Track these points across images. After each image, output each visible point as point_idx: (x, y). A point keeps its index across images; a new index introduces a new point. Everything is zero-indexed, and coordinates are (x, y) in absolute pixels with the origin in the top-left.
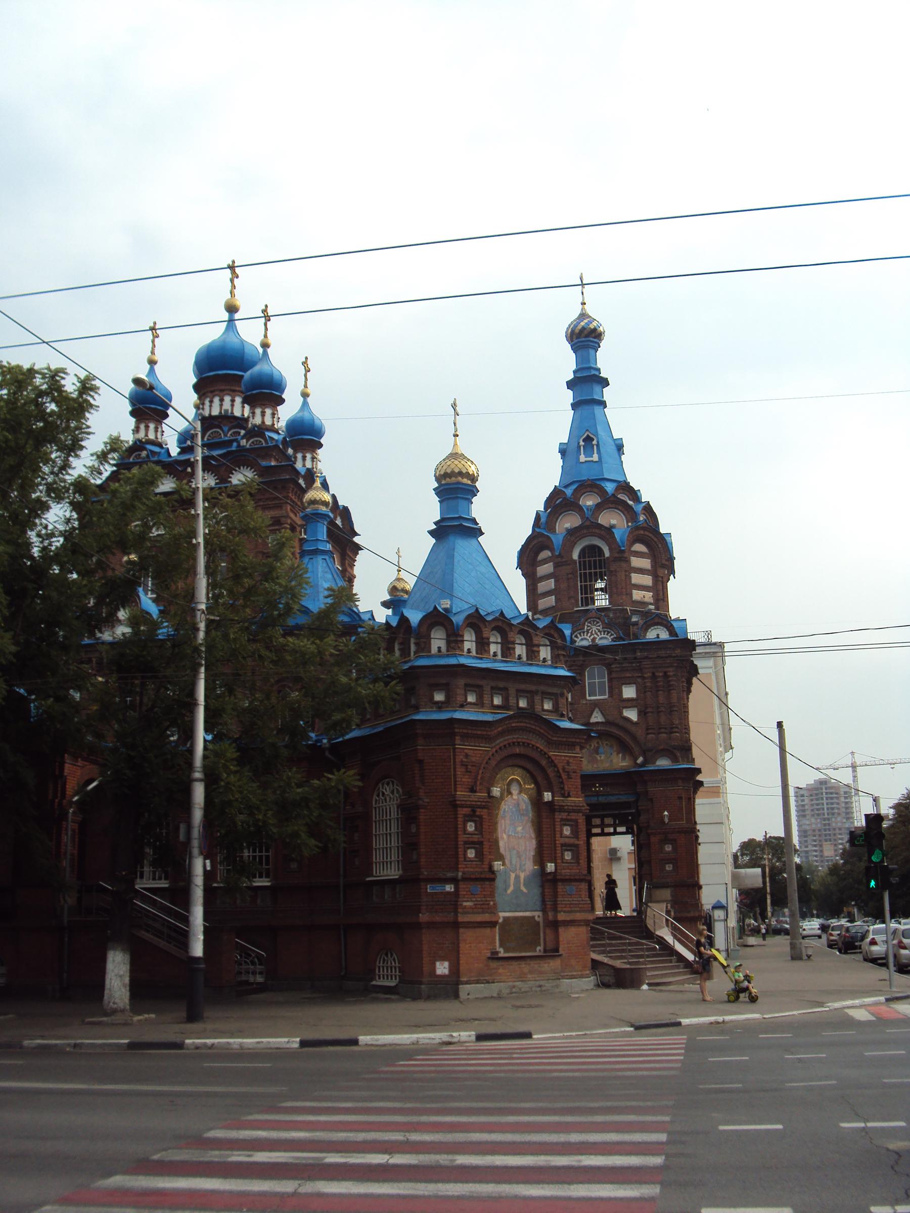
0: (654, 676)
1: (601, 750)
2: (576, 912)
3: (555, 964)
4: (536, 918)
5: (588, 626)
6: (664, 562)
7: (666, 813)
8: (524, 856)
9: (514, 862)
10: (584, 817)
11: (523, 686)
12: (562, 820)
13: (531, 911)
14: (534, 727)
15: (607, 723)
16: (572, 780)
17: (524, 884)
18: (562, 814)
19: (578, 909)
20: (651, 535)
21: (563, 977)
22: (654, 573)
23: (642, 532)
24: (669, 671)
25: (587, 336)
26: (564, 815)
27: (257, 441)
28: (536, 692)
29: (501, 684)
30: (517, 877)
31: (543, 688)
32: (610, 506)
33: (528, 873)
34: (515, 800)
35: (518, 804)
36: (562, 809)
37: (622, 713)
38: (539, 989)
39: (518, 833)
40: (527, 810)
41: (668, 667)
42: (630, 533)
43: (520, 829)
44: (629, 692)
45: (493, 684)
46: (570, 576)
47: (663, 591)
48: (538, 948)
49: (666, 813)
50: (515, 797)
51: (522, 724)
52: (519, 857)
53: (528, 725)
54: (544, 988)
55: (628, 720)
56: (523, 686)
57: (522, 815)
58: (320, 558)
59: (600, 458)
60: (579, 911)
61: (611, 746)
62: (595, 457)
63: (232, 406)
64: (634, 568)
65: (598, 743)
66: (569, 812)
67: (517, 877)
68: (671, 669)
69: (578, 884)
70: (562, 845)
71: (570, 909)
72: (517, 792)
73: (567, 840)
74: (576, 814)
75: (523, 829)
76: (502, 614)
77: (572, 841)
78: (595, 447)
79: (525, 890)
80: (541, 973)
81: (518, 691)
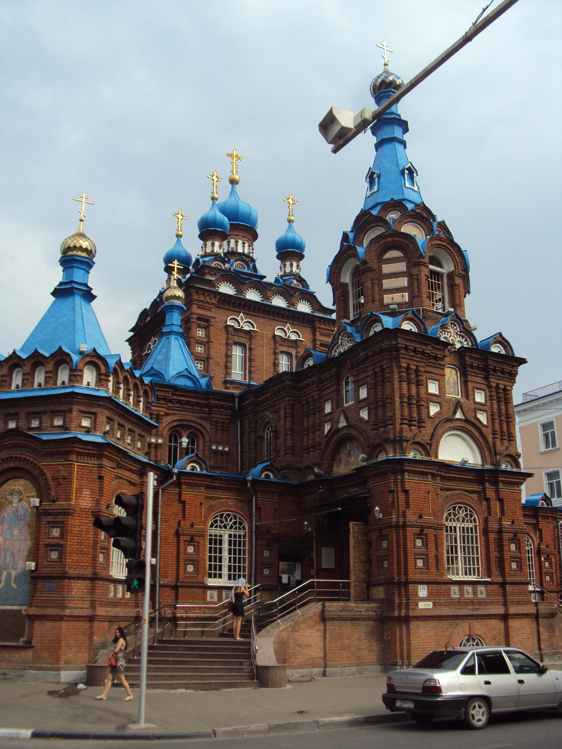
0: (375, 373)
1: (352, 453)
2: (48, 607)
3: (28, 655)
4: (23, 612)
5: (342, 339)
6: (416, 260)
7: (377, 508)
8: (18, 555)
9: (7, 562)
10: (93, 519)
11: (32, 409)
12: (49, 523)
13: (19, 605)
14: (25, 443)
15: (349, 426)
16: (63, 486)
17: (15, 582)
18: (49, 517)
19: (55, 605)
20: (399, 239)
21: (30, 668)
22: (408, 274)
23: (390, 239)
24: (383, 365)
25: (379, 90)
26: (50, 518)
27: (242, 265)
28: (45, 412)
29: (12, 411)
30: (9, 575)
31: (52, 408)
32: (372, 225)
33: (19, 571)
34: (14, 507)
35: (17, 511)
36: (46, 513)
37: (359, 414)
38: (3, 676)
39: (14, 536)
40: (25, 515)
41: (382, 360)
42: (428, 243)
43: (16, 532)
44: (363, 393)
45: (6, 411)
46: (341, 298)
47: (418, 288)
48: (22, 639)
49: (377, 508)
50: (15, 505)
51: (14, 442)
52: (13, 556)
53: (20, 442)
54: (7, 677)
55: (362, 419)
56: (32, 409)
57: (20, 520)
58: (173, 337)
59: (378, 187)
60: (53, 607)
61: (358, 448)
62: (376, 188)
63: (237, 245)
64: (386, 275)
65: (350, 446)
66: (56, 515)
67: (9, 575)
68: (384, 362)
69: (58, 581)
70: (47, 545)
71: (45, 605)
72: (17, 500)
73: (53, 541)
74: (63, 517)
75: (19, 533)
76: (94, 350)
77: (60, 542)
78: (376, 179)
79: (15, 586)
80: (10, 662)
81: (29, 414)
